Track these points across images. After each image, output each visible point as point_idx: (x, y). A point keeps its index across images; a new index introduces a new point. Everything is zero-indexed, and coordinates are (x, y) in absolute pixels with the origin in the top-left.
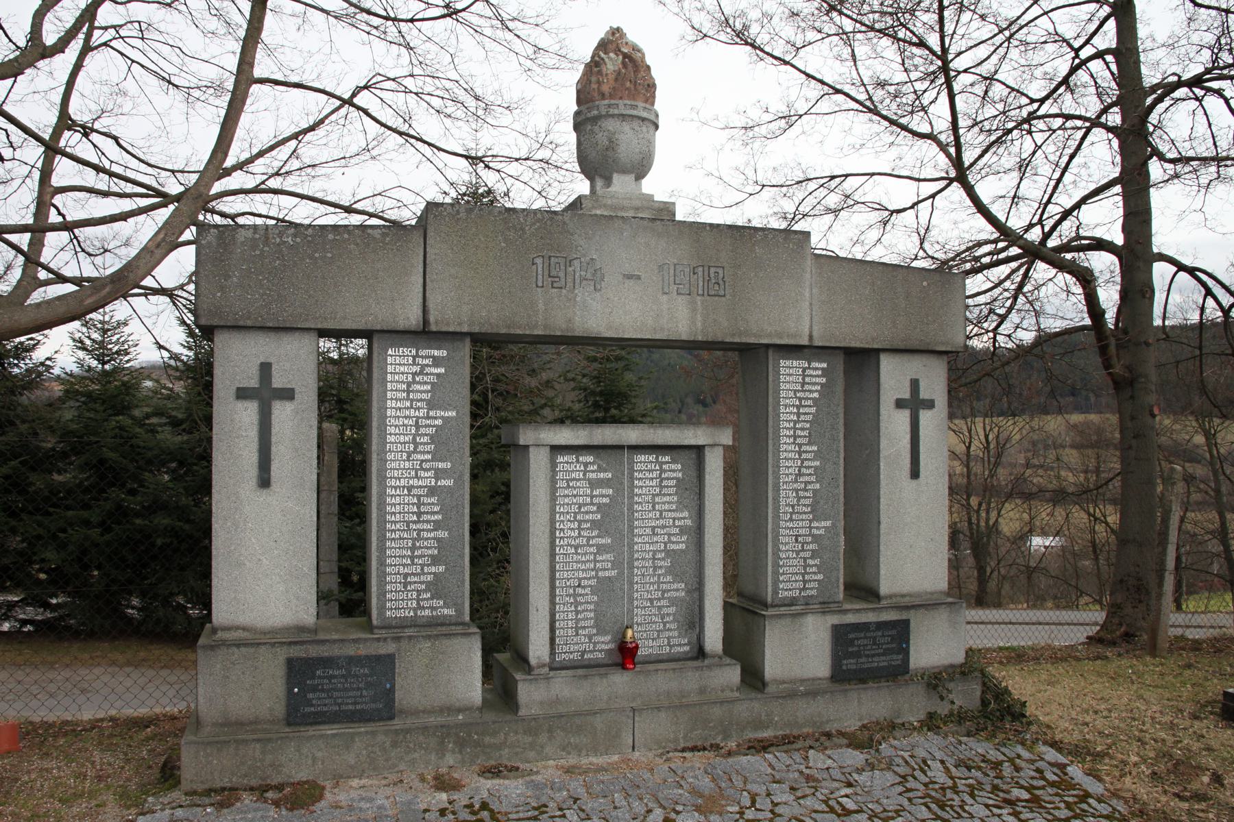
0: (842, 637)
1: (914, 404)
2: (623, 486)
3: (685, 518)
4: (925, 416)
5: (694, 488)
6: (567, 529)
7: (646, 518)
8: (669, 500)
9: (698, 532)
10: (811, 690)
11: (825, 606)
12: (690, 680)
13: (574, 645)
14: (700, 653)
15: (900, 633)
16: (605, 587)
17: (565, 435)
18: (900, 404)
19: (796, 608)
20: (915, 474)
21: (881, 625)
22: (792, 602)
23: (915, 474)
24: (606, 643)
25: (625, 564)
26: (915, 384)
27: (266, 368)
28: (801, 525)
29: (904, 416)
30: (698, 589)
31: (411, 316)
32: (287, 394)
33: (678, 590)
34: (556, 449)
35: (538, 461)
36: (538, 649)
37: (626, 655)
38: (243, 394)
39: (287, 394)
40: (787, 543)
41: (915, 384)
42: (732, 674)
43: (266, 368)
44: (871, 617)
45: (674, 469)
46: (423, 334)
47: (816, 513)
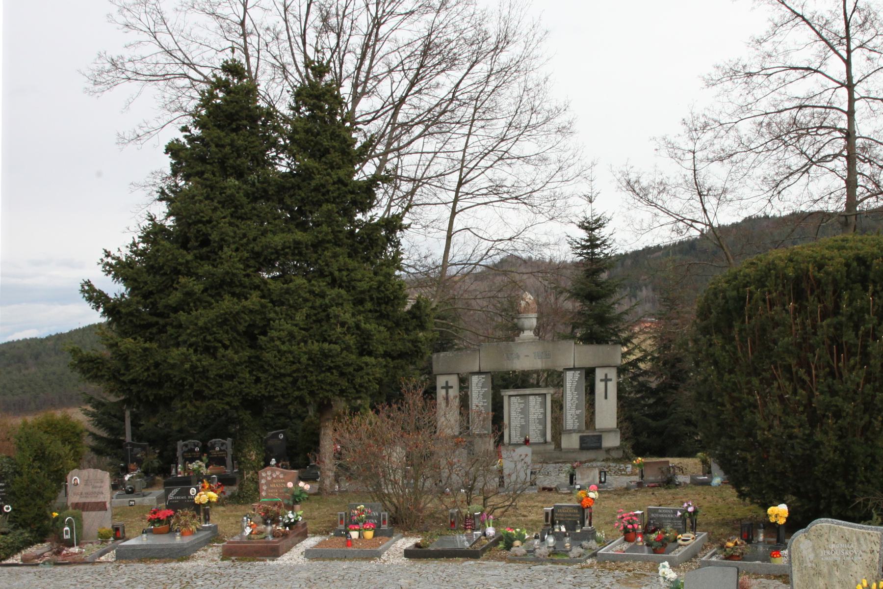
0: (582, 439)
1: (606, 380)
2: (527, 404)
3: (542, 410)
4: (609, 383)
5: (544, 404)
6: (513, 414)
7: (532, 410)
8: (538, 407)
9: (545, 414)
10: (574, 451)
11: (579, 431)
12: (542, 448)
13: (514, 440)
14: (546, 442)
15: (599, 438)
16: (522, 427)
17: (512, 393)
18: (602, 380)
19: (570, 432)
20: (606, 398)
21: (593, 436)
22: (570, 430)
23: (606, 398)
24: (523, 439)
25: (527, 421)
26: (606, 375)
27: (447, 382)
28: (573, 411)
29: (603, 384)
30: (545, 427)
31: (476, 369)
32: (451, 387)
33: (541, 427)
34: (510, 396)
35: (506, 399)
36: (506, 439)
37: (527, 442)
38: (442, 388)
39: (451, 387)
40: (569, 417)
41: (606, 375)
42: (553, 447)
43: (447, 382)
44: (591, 434)
45: (539, 399)
46: (479, 373)
47: (577, 408)
